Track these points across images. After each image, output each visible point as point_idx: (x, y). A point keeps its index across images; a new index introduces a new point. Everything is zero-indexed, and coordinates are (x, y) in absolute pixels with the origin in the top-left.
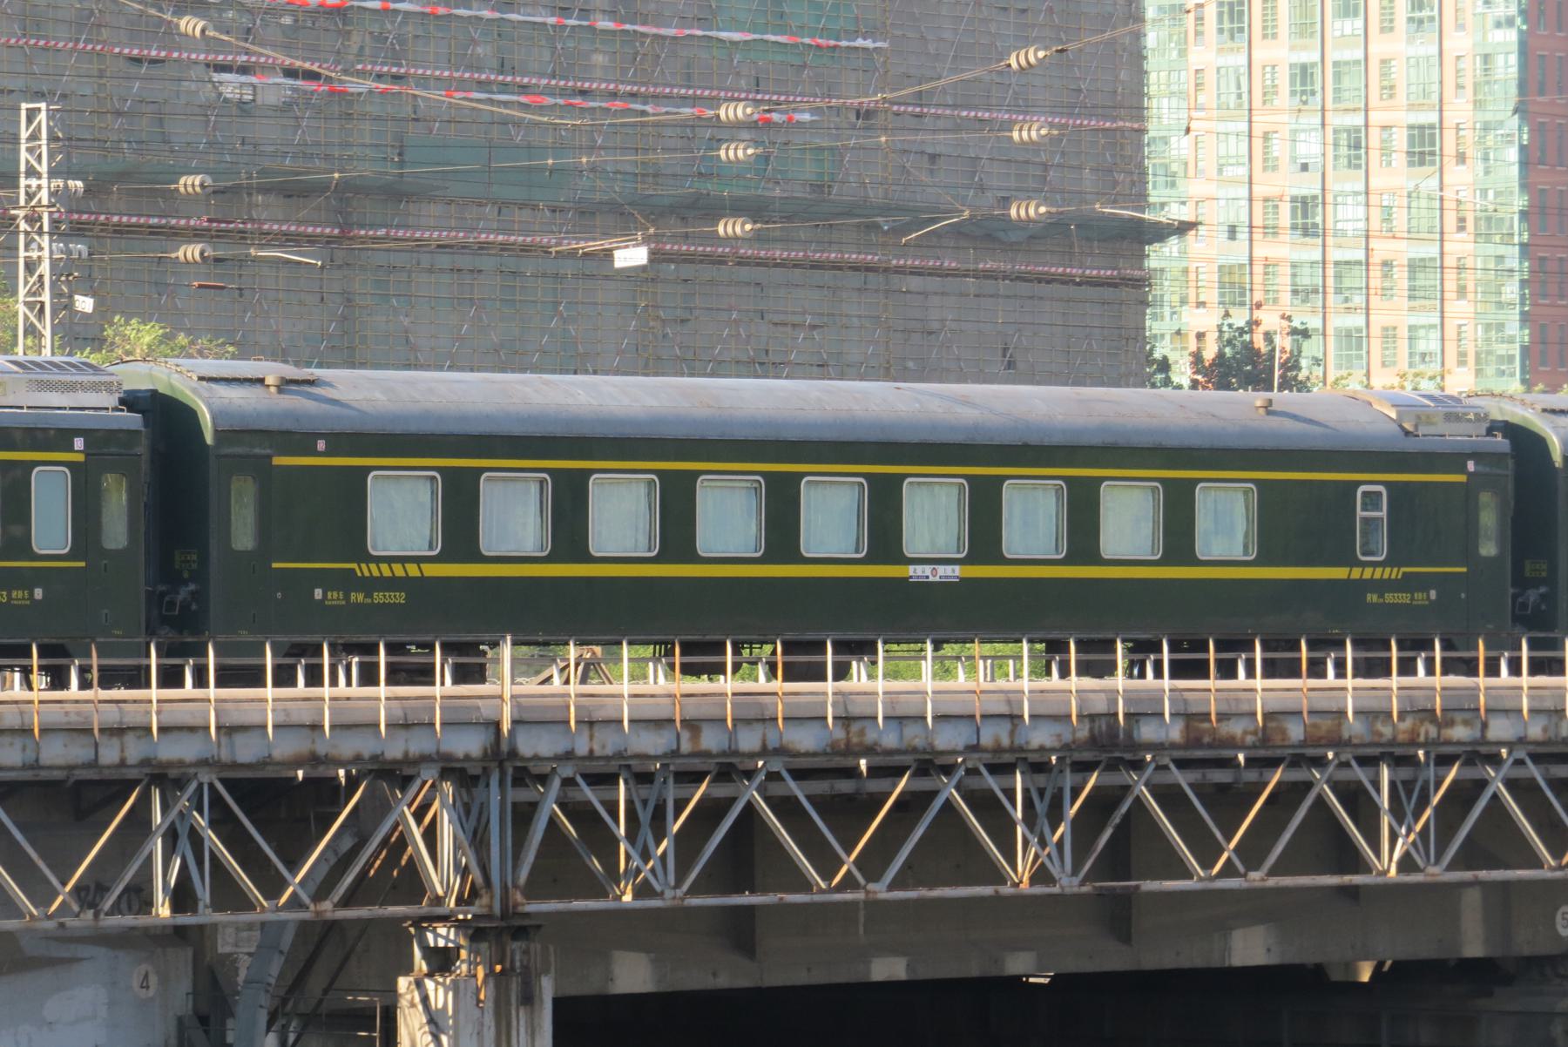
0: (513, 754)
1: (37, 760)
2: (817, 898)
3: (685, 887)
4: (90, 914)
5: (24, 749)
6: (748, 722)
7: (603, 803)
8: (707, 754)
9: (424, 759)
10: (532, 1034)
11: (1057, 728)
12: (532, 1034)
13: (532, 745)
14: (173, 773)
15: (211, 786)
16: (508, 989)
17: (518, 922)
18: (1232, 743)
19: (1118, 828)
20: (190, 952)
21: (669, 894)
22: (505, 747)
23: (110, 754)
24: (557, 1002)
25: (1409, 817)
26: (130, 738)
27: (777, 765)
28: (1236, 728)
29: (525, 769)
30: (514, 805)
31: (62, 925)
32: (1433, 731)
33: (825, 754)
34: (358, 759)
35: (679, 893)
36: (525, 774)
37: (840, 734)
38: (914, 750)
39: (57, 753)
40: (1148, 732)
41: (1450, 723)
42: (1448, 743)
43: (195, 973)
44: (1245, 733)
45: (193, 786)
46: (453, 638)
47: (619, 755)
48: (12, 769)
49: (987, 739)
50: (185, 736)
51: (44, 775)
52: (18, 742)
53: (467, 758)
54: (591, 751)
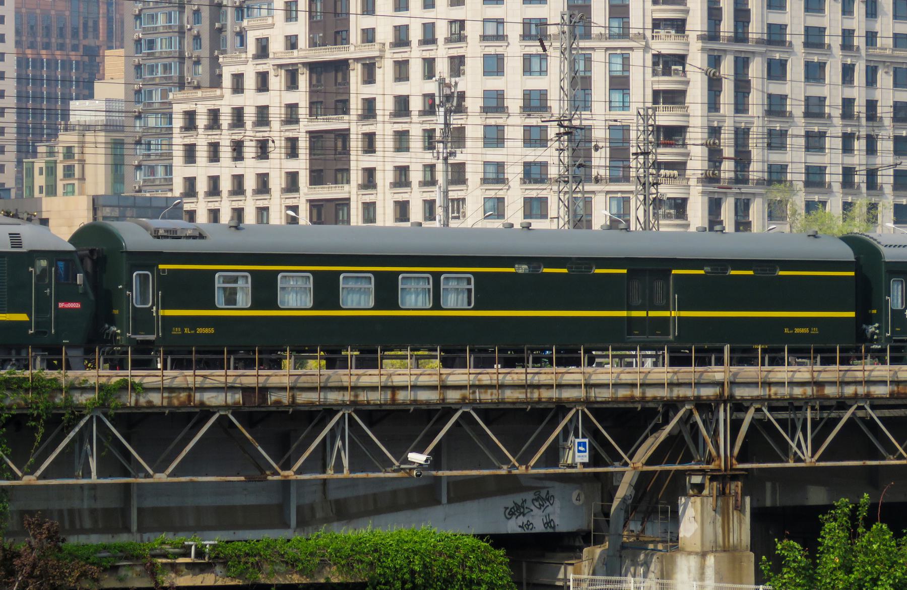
0: (732, 397)
2: (883, 463)
4: (524, 467)
5: (492, 394)
6: (848, 383)
7: (777, 420)
8: (828, 398)
10: (740, 523)
12: (740, 523)
14: (568, 406)
15: (583, 412)
20: (600, 486)
21: (808, 460)
22: (726, 394)
24: (752, 509)
29: (741, 404)
30: (731, 420)
31: (510, 472)
33: (886, 398)
34: (654, 399)
35: (814, 460)
36: (739, 406)
43: (602, 493)
45: (574, 411)
46: (616, 345)
47: (782, 399)
48: (486, 403)
51: (501, 406)
52: (489, 391)
54: (770, 396)
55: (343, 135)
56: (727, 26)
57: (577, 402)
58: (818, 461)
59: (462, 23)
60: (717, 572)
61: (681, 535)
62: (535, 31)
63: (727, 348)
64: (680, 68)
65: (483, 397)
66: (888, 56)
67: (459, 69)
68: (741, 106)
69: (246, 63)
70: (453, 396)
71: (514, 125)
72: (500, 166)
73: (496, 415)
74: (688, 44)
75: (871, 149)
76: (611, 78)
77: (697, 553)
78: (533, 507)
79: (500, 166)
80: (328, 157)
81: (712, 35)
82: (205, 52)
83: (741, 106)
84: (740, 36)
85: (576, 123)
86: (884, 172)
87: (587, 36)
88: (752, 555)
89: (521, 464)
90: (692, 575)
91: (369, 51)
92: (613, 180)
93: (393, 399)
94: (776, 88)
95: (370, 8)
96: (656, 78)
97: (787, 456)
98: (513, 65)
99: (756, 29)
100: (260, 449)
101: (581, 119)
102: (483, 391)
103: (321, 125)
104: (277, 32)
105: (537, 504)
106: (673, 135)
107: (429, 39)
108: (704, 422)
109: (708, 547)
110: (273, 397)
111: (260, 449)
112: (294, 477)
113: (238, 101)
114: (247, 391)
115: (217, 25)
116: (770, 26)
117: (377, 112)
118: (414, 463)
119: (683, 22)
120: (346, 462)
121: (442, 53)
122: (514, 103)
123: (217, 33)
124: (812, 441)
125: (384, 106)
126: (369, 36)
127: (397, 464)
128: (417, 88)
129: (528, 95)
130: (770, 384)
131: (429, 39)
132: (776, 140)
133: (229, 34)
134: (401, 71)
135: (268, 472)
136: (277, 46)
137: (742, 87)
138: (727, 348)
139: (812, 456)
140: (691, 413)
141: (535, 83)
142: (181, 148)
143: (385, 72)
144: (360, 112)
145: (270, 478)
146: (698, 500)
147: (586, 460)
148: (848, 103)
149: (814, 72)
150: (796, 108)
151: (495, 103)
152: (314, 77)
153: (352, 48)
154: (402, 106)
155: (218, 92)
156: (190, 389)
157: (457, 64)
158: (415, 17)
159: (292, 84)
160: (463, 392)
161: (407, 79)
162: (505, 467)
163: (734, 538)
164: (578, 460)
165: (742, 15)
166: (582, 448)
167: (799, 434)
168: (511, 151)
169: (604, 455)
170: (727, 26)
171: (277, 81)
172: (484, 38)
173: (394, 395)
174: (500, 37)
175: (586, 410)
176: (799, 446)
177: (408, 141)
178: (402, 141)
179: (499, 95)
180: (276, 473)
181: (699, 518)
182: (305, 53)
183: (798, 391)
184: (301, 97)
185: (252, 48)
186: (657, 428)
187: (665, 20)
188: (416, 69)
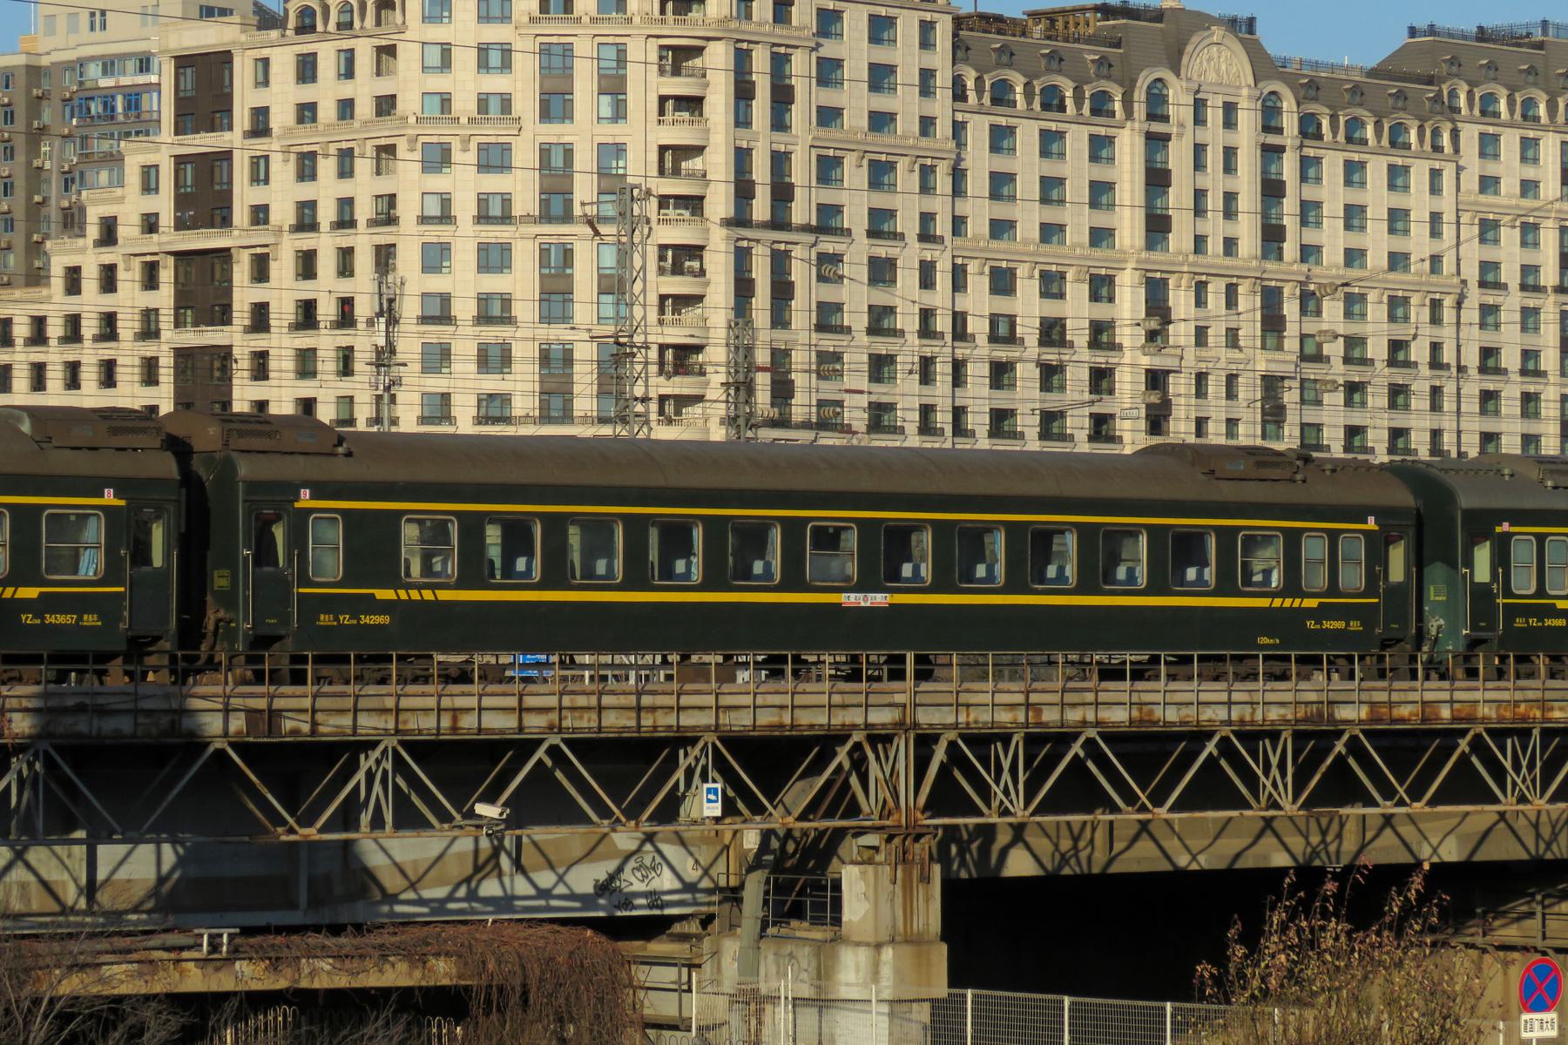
0: (916, 725)
1: (600, 727)
3: (1031, 809)
6: (1074, 705)
8: (1045, 725)
9: (854, 727)
11: (1282, 711)
13: (926, 717)
15: (714, 745)
16: (911, 874)
17: (918, 830)
18: (1402, 720)
19: (1324, 775)
21: (1020, 813)
23: (647, 721)
25: (1524, 770)
26: (659, 713)
27: (1092, 733)
28: (1404, 711)
32: (1538, 714)
34: (812, 726)
37: (1135, 714)
38: (1183, 723)
39: (612, 720)
40: (1345, 713)
41: (1552, 709)
42: (1550, 720)
44: (1411, 714)
45: (701, 744)
49: (1234, 717)
50: (696, 712)
52: (586, 716)
53: (884, 726)
55: (224, 355)
56: (761, 208)
57: (707, 729)
58: (1032, 814)
59: (394, 196)
60: (897, 971)
61: (845, 918)
62: (493, 211)
63: (910, 657)
64: (696, 264)
65: (577, 725)
66: (981, 250)
67: (387, 264)
68: (780, 319)
69: (83, 250)
70: (534, 722)
71: (465, 341)
72: (446, 397)
73: (594, 749)
74: (708, 230)
75: (958, 378)
76: (600, 276)
77: (868, 945)
78: (633, 879)
79: (446, 397)
80: (284, 383)
81: (740, 220)
82: (18, 238)
83: (780, 319)
84: (779, 222)
85: (638, 339)
86: (1075, 412)
87: (567, 217)
88: (944, 947)
89: (629, 818)
90: (861, 974)
91: (260, 237)
92: (602, 420)
93: (455, 729)
94: (828, 293)
95: (262, 176)
96: (662, 278)
97: (989, 807)
98: (464, 254)
99: (801, 211)
100: (270, 797)
101: (646, 334)
102: (577, 714)
103: (193, 338)
104: (129, 206)
105: (639, 875)
106: (683, 358)
107: (345, 222)
108: (878, 758)
109: (884, 937)
110: (288, 725)
111: (270, 797)
112: (318, 837)
113: (72, 304)
114: (251, 713)
115: (37, 198)
116: (822, 208)
117: (272, 322)
118: (480, 816)
119: (702, 198)
120: (388, 817)
121: (364, 242)
122: (464, 309)
123: (35, 211)
124: (1026, 783)
125: (283, 310)
126: (260, 214)
127: (458, 817)
128: (326, 289)
129: (484, 300)
130: (968, 706)
131: (345, 222)
132: (828, 364)
133: (53, 212)
134: (307, 265)
135: (280, 830)
136: (128, 230)
137: (782, 291)
138: (910, 657)
139: (1026, 807)
140: (858, 746)
141: (494, 283)
142: (60, 368)
143: (283, 267)
144: (247, 322)
145: (284, 838)
146: (870, 869)
147: (718, 813)
148: (927, 315)
149: (881, 271)
150: (857, 319)
151: (439, 312)
152: (181, 270)
153: (236, 233)
154: (307, 315)
155: (45, 292)
156: (175, 711)
157: (385, 257)
158: (326, 190)
159: (150, 279)
160: (554, 716)
161: (352, 275)
162: (606, 822)
163: (918, 924)
164: (707, 813)
165: (782, 193)
166: (712, 797)
167: (1006, 776)
168: (519, 377)
169: (740, 805)
170: (761, 208)
171: (128, 278)
172: (423, 220)
173: (455, 720)
174: (446, 218)
175: (718, 744)
176: (1006, 792)
177: (315, 361)
178: (306, 364)
179: (445, 299)
180: (292, 831)
181: (871, 894)
182: (171, 239)
183: (1004, 717)
184: (164, 298)
185: (93, 232)
186: (816, 768)
187: (677, 197)
188: (327, 264)
